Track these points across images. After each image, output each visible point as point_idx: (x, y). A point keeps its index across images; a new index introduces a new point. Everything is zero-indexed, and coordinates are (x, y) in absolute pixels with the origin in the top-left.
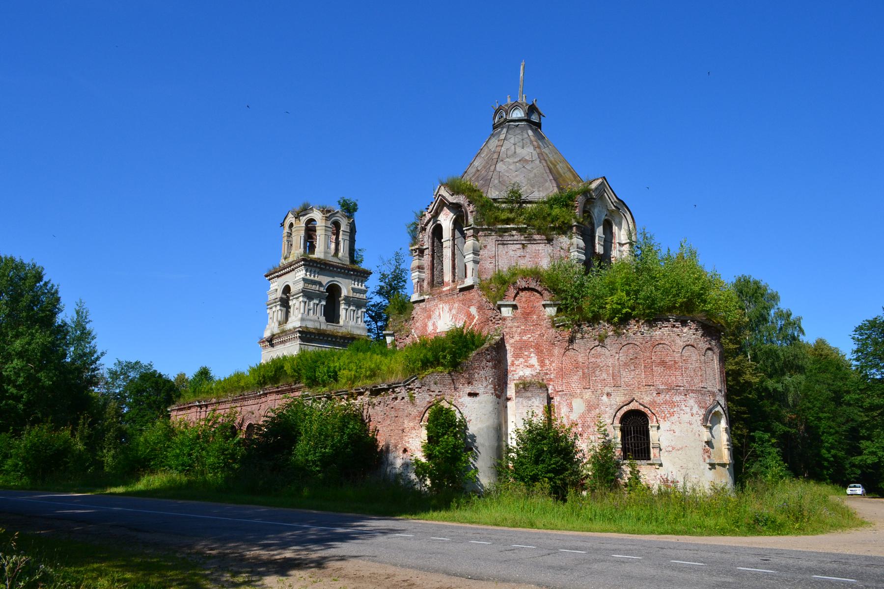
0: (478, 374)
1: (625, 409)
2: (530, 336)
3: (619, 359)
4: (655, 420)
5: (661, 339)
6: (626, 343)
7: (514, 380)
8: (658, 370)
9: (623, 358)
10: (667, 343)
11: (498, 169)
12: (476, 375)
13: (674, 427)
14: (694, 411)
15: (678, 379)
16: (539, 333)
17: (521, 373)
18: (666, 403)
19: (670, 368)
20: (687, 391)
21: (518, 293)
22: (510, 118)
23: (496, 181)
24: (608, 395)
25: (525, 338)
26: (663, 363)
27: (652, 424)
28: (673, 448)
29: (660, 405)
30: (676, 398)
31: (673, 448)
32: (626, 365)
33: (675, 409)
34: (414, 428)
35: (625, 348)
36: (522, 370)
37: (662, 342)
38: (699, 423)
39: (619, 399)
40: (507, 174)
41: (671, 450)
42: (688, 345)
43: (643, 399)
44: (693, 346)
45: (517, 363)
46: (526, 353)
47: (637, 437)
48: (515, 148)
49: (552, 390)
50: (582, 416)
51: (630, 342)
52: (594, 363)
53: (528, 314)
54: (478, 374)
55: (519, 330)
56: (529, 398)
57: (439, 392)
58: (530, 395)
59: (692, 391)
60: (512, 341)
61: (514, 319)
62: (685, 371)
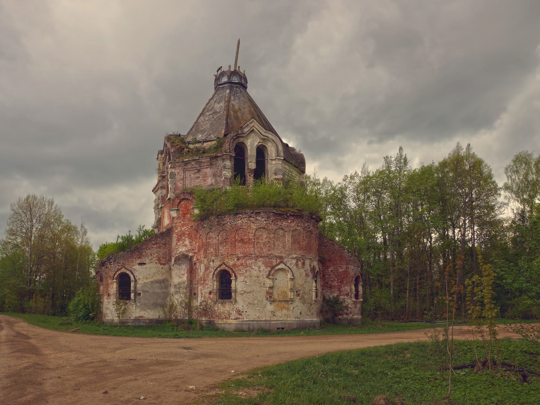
0: (145, 252)
1: (219, 269)
2: (185, 227)
3: (218, 239)
4: (234, 275)
5: (241, 226)
6: (222, 229)
7: (177, 254)
8: (239, 245)
9: (220, 239)
10: (245, 227)
12: (144, 253)
13: (246, 280)
14: (262, 269)
15: (250, 249)
16: (190, 225)
17: (181, 250)
18: (242, 265)
19: (246, 243)
20: (257, 256)
21: (180, 202)
22: (220, 83)
23: (194, 130)
24: (213, 261)
26: (242, 241)
27: (233, 278)
28: (245, 292)
30: (249, 262)
31: (245, 292)
32: (222, 243)
33: (248, 269)
34: (111, 283)
35: (221, 233)
36: (181, 248)
37: (242, 227)
38: (265, 276)
39: (217, 263)
40: (202, 124)
41: (243, 293)
42: (260, 228)
43: (229, 263)
44: (264, 228)
45: (178, 244)
46: (183, 238)
47: (226, 285)
48: (214, 104)
49: (196, 259)
50: (204, 275)
51: (224, 228)
52: (208, 242)
54: (145, 252)
55: (180, 224)
56: (180, 265)
57: (123, 263)
58: (181, 263)
59: (261, 257)
61: (178, 218)
62: (257, 245)
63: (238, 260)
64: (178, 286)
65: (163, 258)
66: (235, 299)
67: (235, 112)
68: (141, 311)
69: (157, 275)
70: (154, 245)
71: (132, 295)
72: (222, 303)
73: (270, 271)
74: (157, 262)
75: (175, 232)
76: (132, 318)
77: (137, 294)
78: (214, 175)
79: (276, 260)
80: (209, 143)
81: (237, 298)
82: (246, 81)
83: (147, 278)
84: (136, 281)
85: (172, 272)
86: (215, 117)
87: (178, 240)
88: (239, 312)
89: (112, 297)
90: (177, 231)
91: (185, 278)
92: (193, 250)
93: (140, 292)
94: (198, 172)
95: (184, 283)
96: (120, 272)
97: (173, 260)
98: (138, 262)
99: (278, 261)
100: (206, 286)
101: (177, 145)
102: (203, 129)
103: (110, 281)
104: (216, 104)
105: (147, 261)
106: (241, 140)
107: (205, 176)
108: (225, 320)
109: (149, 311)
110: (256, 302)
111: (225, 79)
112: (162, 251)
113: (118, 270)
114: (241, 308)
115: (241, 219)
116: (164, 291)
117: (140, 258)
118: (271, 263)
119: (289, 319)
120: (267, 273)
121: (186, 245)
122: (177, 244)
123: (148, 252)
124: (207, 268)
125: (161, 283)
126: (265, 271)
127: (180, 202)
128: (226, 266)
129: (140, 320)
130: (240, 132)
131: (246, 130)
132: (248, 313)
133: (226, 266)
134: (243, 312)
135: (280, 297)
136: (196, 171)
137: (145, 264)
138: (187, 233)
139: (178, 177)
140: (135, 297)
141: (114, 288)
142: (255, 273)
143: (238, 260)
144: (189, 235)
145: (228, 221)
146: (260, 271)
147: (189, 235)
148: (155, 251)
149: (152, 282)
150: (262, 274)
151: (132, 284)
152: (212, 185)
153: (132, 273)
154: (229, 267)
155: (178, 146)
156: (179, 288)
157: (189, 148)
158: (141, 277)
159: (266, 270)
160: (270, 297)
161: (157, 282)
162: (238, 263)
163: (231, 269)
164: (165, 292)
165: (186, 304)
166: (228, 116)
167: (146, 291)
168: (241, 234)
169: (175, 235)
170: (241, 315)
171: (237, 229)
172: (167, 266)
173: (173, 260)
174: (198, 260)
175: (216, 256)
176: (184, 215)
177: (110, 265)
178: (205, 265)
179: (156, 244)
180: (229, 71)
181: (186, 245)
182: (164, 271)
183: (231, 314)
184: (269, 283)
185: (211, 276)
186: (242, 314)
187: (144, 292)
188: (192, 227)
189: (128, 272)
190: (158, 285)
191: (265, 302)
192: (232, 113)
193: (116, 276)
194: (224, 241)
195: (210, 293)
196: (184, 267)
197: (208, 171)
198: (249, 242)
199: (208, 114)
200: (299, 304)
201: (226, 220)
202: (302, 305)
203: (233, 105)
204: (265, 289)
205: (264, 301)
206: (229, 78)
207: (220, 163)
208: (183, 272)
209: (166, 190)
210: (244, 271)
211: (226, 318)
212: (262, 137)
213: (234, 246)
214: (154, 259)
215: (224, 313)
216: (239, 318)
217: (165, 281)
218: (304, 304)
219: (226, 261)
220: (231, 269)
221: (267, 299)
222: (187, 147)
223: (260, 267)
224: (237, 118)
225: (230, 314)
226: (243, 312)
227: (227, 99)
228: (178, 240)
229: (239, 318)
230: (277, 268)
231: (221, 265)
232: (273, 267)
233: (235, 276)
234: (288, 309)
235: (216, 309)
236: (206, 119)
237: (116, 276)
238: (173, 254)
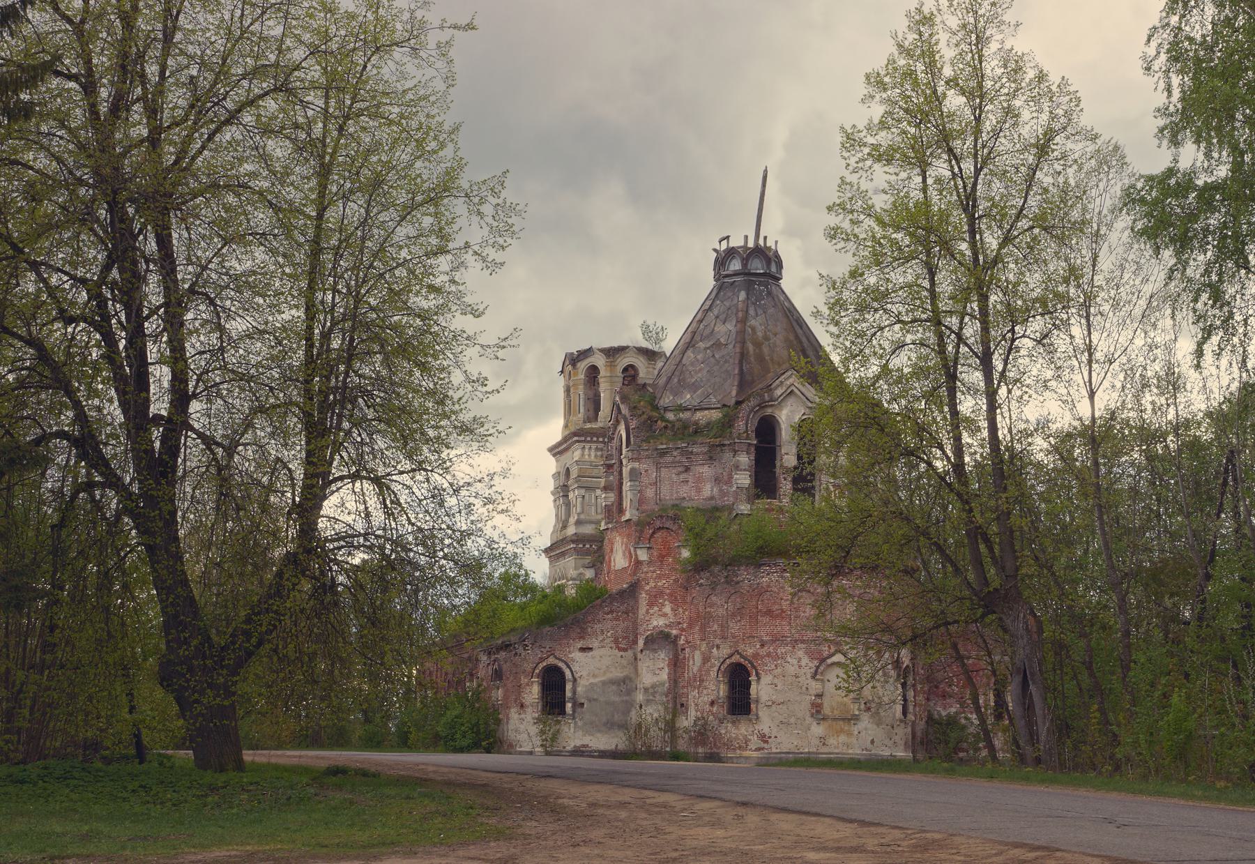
1: (728, 662)
5: (769, 586)
11: (684, 361)
12: (589, 629)
13: (776, 681)
14: (803, 663)
15: (784, 628)
17: (655, 623)
18: (769, 655)
19: (777, 616)
20: (796, 641)
21: (654, 533)
23: (676, 380)
24: (718, 647)
25: (659, 584)
26: (769, 613)
27: (753, 678)
29: (762, 657)
30: (781, 650)
31: (773, 703)
32: (734, 615)
34: (528, 685)
35: (733, 597)
38: (809, 676)
39: (725, 651)
45: (651, 611)
50: (700, 670)
52: (709, 612)
53: (663, 557)
55: (655, 575)
56: (655, 651)
59: (803, 642)
60: (647, 588)
61: (650, 563)
63: (762, 646)
64: (651, 691)
65: (624, 638)
66: (757, 715)
67: (758, 345)
68: (584, 735)
69: (613, 669)
70: (608, 614)
71: (569, 706)
72: (733, 723)
73: (818, 667)
74: (613, 645)
75: (643, 589)
76: (568, 748)
77: (578, 705)
78: (717, 480)
79: (829, 647)
80: (706, 412)
81: (760, 714)
82: (780, 265)
83: (594, 676)
84: (575, 680)
85: (640, 664)
86: (717, 356)
87: (651, 605)
88: (764, 738)
89: (529, 710)
90: (647, 588)
91: (664, 676)
92: (679, 623)
93: (583, 701)
94: (686, 471)
95: (663, 684)
96: (545, 664)
97: (641, 643)
98: (579, 645)
99: (833, 649)
100: (705, 692)
101: (643, 413)
102: (693, 380)
103: (524, 680)
104: (718, 325)
105: (595, 643)
106: (769, 411)
107: (699, 479)
108: (738, 751)
109: (599, 735)
110: (792, 720)
111: (736, 265)
112: (622, 625)
113: (542, 660)
114: (766, 731)
115: (768, 574)
116: (624, 698)
117: (582, 638)
118: (820, 652)
119: (850, 751)
120: (813, 670)
121: (665, 615)
122: (647, 612)
123: (598, 627)
124: (706, 659)
125: (619, 685)
126: (808, 664)
127: (654, 533)
128: (742, 656)
129: (583, 752)
130: (766, 397)
131: (779, 392)
132: (779, 740)
133: (742, 656)
134: (770, 737)
135: (835, 712)
136: (680, 469)
137: (591, 649)
138: (668, 591)
139: (645, 480)
140: (574, 711)
141: (533, 692)
142: (791, 670)
143: (762, 646)
144: (671, 595)
145: (745, 575)
146: (800, 667)
147: (671, 595)
148: (609, 625)
149: (604, 683)
150: (803, 671)
151: (569, 687)
152: (712, 498)
153: (569, 667)
154: (745, 658)
155: (645, 416)
156: (654, 694)
157: (667, 421)
158: (584, 673)
159: (810, 664)
160: (818, 712)
161: (613, 682)
162: (763, 652)
163: (750, 662)
164: (627, 701)
165: (667, 723)
166: (743, 356)
167: (594, 700)
168: (768, 600)
169: (644, 595)
170: (766, 742)
171: (761, 592)
172: (630, 653)
173: (641, 643)
174: (688, 642)
175: (724, 638)
176: (662, 557)
177: (525, 649)
178: (703, 654)
179: (611, 612)
180: (745, 247)
181: (665, 615)
182: (624, 662)
183: (750, 740)
184: (815, 686)
185: (713, 674)
186: (770, 740)
187: (590, 701)
188: (676, 581)
189: (561, 665)
190: (614, 687)
191: (809, 720)
192: (751, 347)
193: (537, 671)
194: (738, 613)
195: (712, 703)
196: (662, 656)
197: (706, 471)
198: (781, 615)
199: (701, 345)
200: (870, 726)
201: (741, 575)
202: (875, 727)
203: (753, 329)
204: (808, 697)
205: (807, 718)
206: (745, 265)
207: (728, 455)
208: (662, 665)
209: (616, 492)
210: (773, 666)
211: (740, 747)
212: (810, 405)
213: (754, 619)
214: (608, 641)
215: (736, 738)
216: (763, 749)
217: (627, 682)
218: (878, 725)
219: (741, 647)
220: (750, 662)
221: (812, 716)
222: (663, 419)
223: (800, 660)
224: (760, 358)
225: (747, 741)
226: (770, 737)
227: (740, 314)
228: (651, 605)
229: (763, 749)
230: (829, 661)
231: (730, 656)
232: (823, 660)
233: (757, 674)
234: (849, 734)
235: (723, 732)
236: (699, 357)
237: (537, 671)
238: (641, 630)
